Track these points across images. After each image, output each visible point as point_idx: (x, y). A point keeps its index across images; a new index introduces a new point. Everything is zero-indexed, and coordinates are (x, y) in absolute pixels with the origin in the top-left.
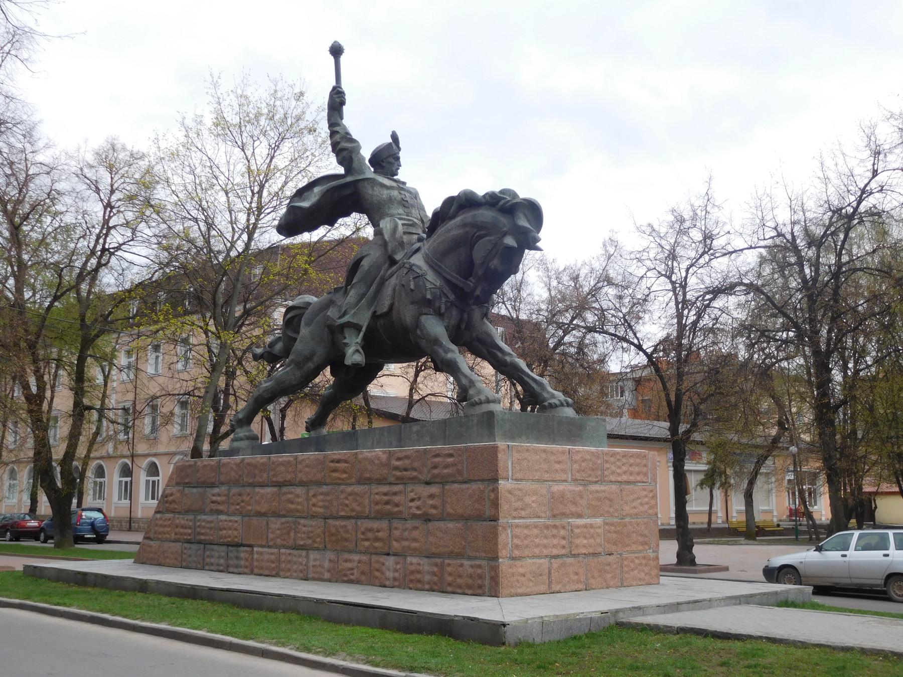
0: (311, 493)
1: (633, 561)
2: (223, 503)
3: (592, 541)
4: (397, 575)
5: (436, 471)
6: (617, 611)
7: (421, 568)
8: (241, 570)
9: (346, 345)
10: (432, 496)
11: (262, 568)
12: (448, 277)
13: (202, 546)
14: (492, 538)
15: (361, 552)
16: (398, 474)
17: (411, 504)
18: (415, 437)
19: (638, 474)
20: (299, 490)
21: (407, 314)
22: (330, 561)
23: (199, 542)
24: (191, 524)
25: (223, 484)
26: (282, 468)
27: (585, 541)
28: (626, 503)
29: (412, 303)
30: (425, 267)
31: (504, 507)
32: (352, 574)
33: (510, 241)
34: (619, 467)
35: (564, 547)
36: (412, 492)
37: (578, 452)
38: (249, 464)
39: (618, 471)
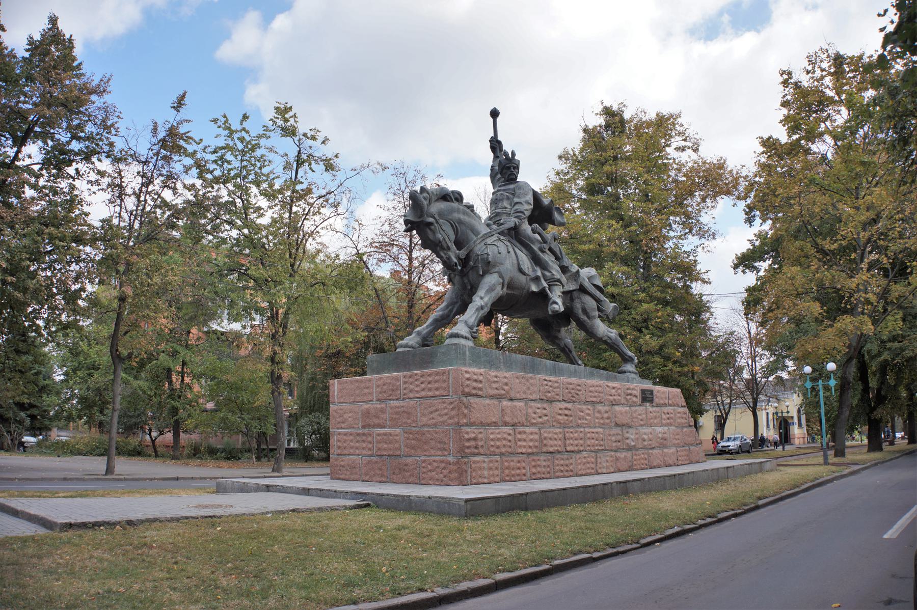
27: (385, 446)
28: (424, 415)
34: (417, 386)
35: (370, 449)
37: (381, 378)
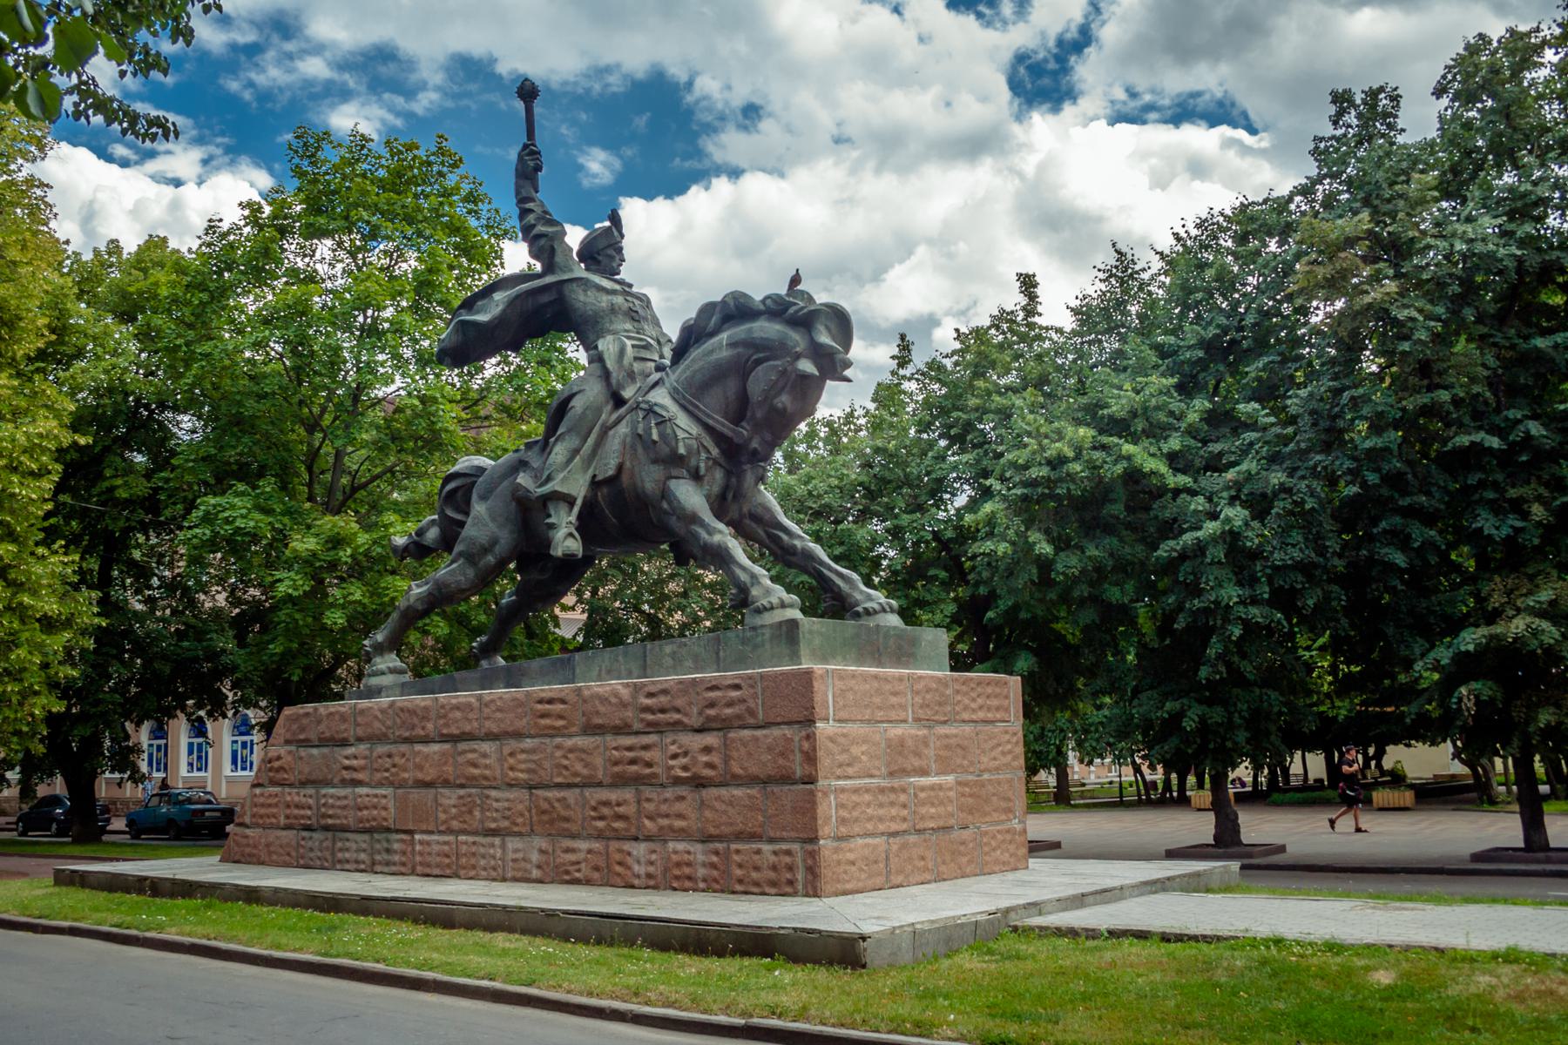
0: (506, 750)
1: (994, 837)
2: (363, 768)
3: (941, 810)
4: (651, 869)
5: (712, 712)
6: (1008, 911)
7: (691, 858)
8: (394, 869)
9: (552, 526)
10: (707, 750)
11: (429, 865)
12: (710, 422)
13: (330, 834)
14: (808, 809)
15: (589, 837)
16: (650, 717)
17: (671, 763)
18: (668, 661)
19: (998, 709)
20: (486, 747)
21: (649, 478)
22: (542, 851)
23: (326, 828)
24: (310, 801)
25: (360, 740)
26: (458, 714)
27: (933, 810)
29: (655, 462)
30: (673, 408)
31: (824, 762)
32: (579, 871)
33: (806, 366)
34: (974, 700)
35: (905, 820)
36: (674, 743)
37: (920, 677)
38: (402, 710)
39: (973, 705)
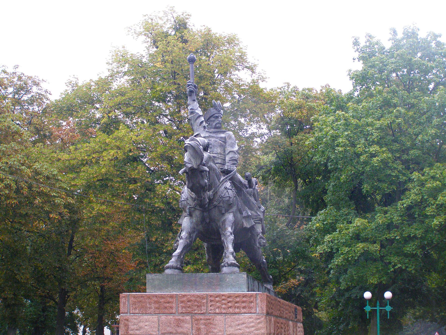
28: (231, 326)
